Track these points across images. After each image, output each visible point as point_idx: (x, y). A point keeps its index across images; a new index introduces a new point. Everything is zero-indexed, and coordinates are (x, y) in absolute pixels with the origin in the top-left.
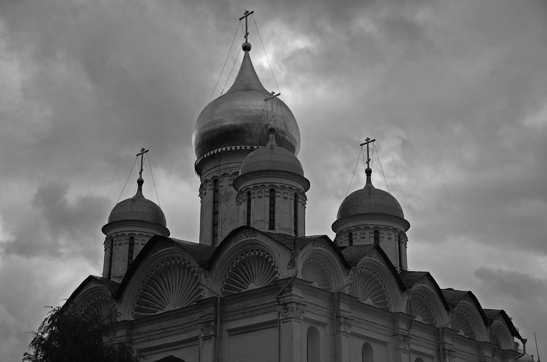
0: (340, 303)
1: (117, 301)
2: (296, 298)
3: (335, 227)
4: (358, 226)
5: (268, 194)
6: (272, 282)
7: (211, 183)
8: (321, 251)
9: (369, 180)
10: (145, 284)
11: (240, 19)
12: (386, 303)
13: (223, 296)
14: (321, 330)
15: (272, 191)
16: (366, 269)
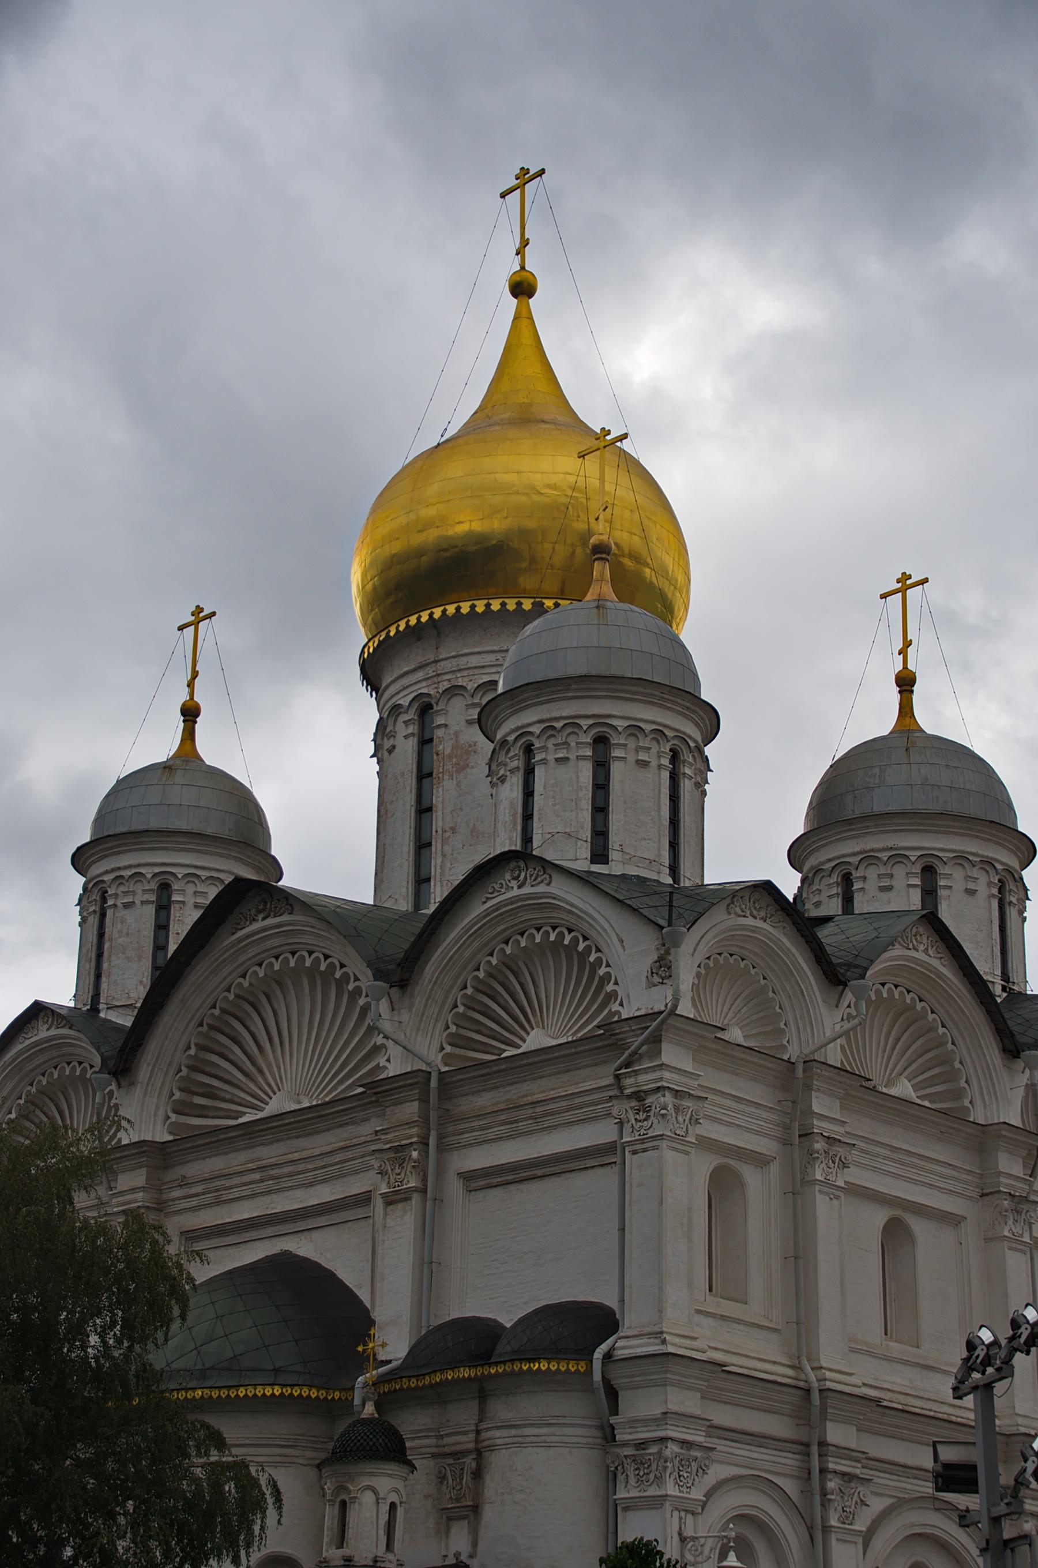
0: (813, 1093)
1: (117, 1080)
2: (675, 1077)
3: (796, 855)
4: (872, 850)
5: (589, 752)
6: (598, 1027)
7: (411, 715)
8: (753, 931)
9: (906, 709)
10: (205, 1029)
11: (503, 196)
12: (958, 1094)
13: (447, 1069)
14: (751, 1176)
15: (601, 742)
16: (896, 986)
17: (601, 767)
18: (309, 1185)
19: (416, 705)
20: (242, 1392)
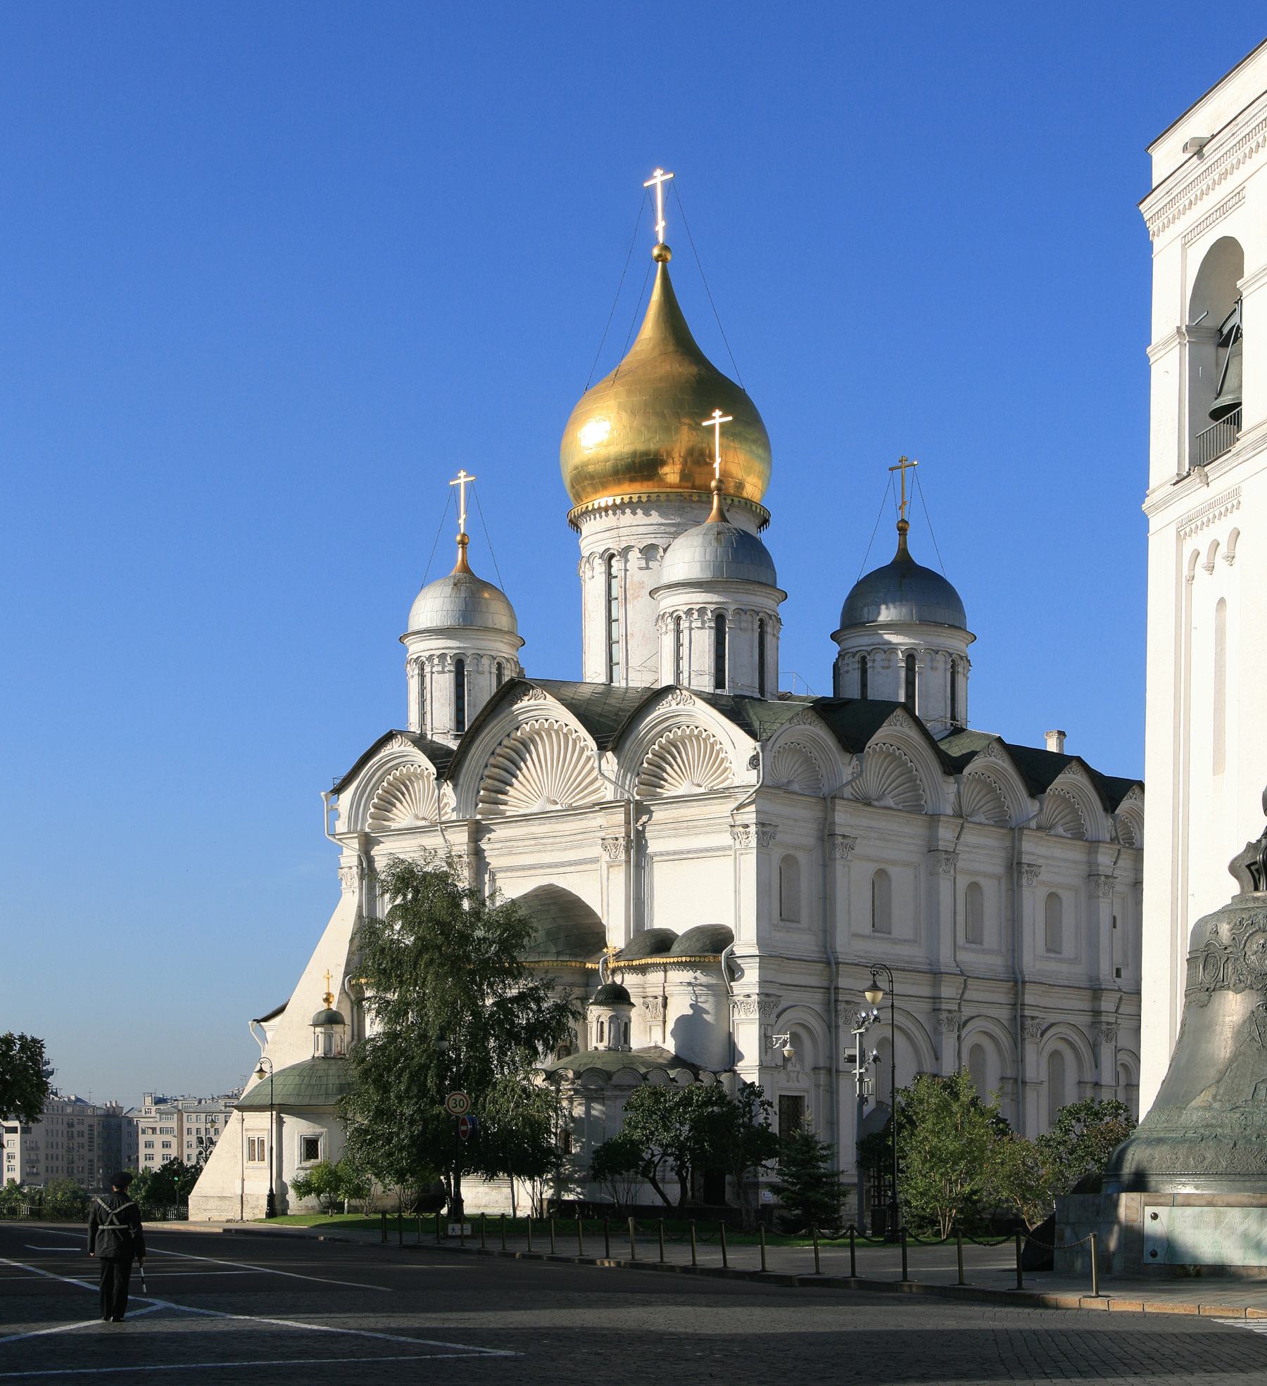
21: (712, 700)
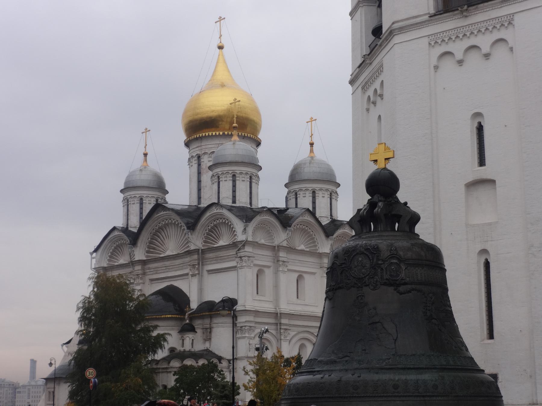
2: (248, 253)
4: (301, 188)
7: (196, 158)
9: (312, 151)
10: (152, 235)
11: (216, 23)
12: (316, 246)
14: (267, 271)
15: (234, 176)
17: (234, 181)
18: (176, 271)
19: (197, 156)
20: (163, 316)
21: (230, 209)
